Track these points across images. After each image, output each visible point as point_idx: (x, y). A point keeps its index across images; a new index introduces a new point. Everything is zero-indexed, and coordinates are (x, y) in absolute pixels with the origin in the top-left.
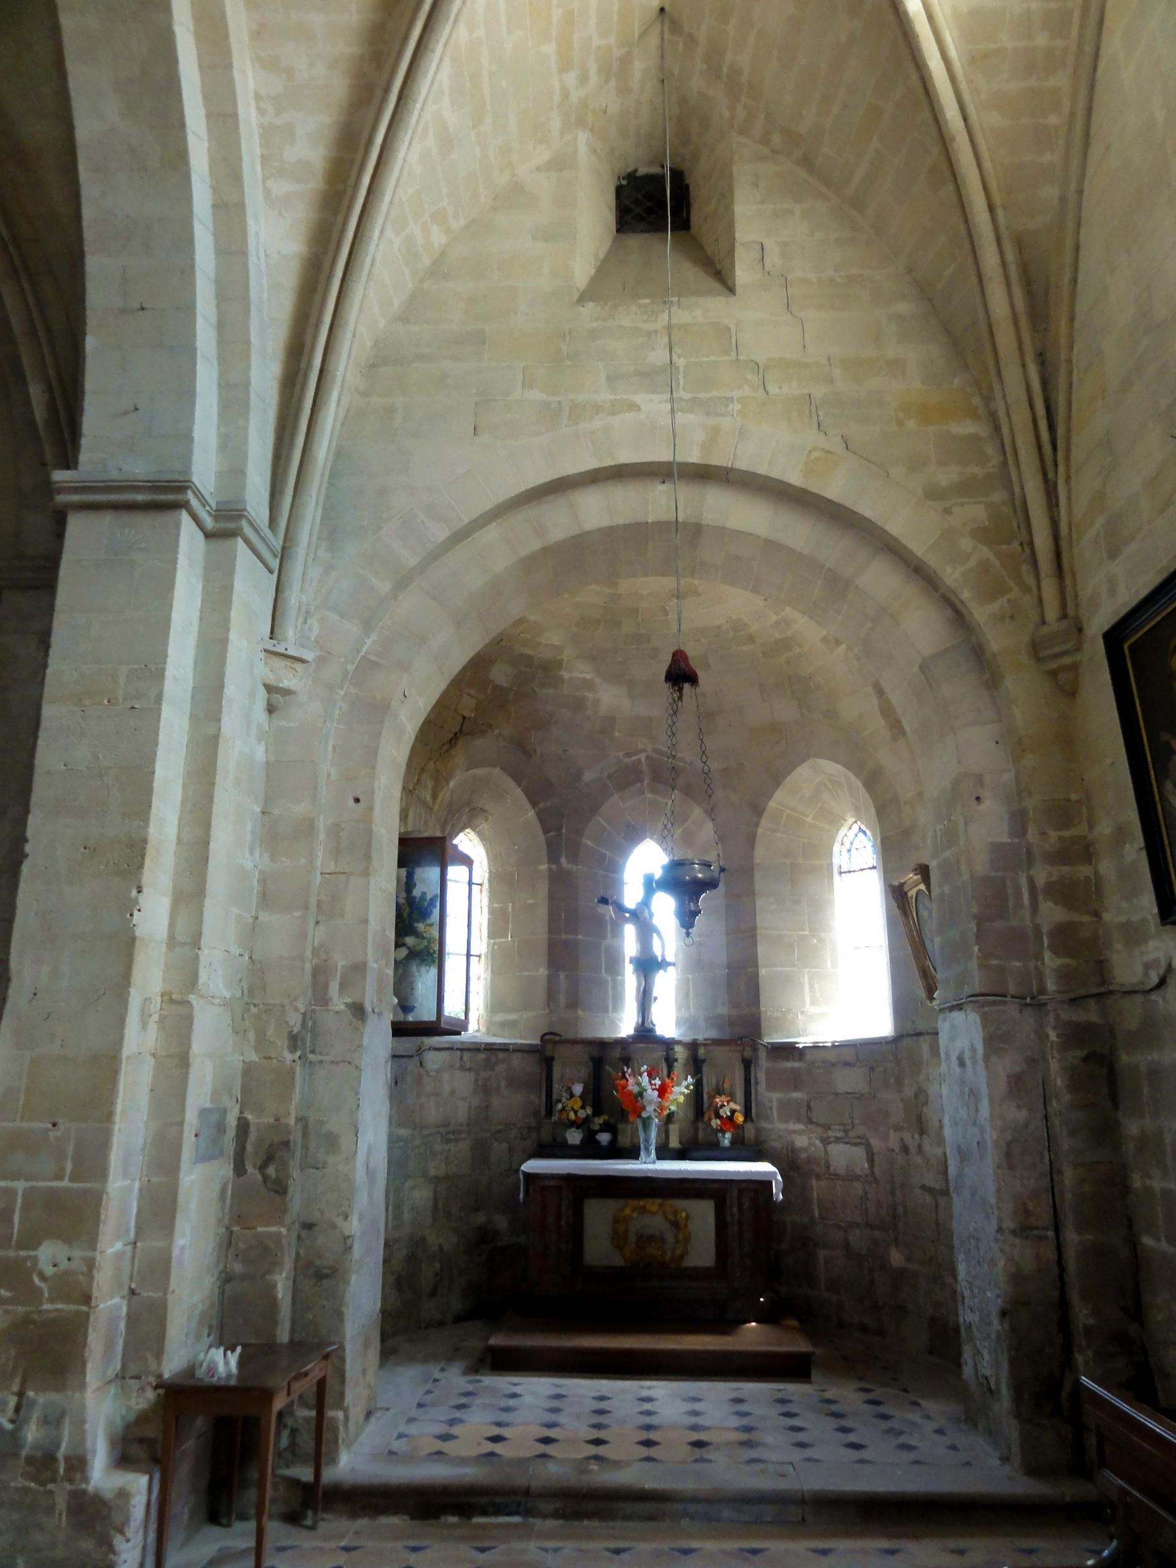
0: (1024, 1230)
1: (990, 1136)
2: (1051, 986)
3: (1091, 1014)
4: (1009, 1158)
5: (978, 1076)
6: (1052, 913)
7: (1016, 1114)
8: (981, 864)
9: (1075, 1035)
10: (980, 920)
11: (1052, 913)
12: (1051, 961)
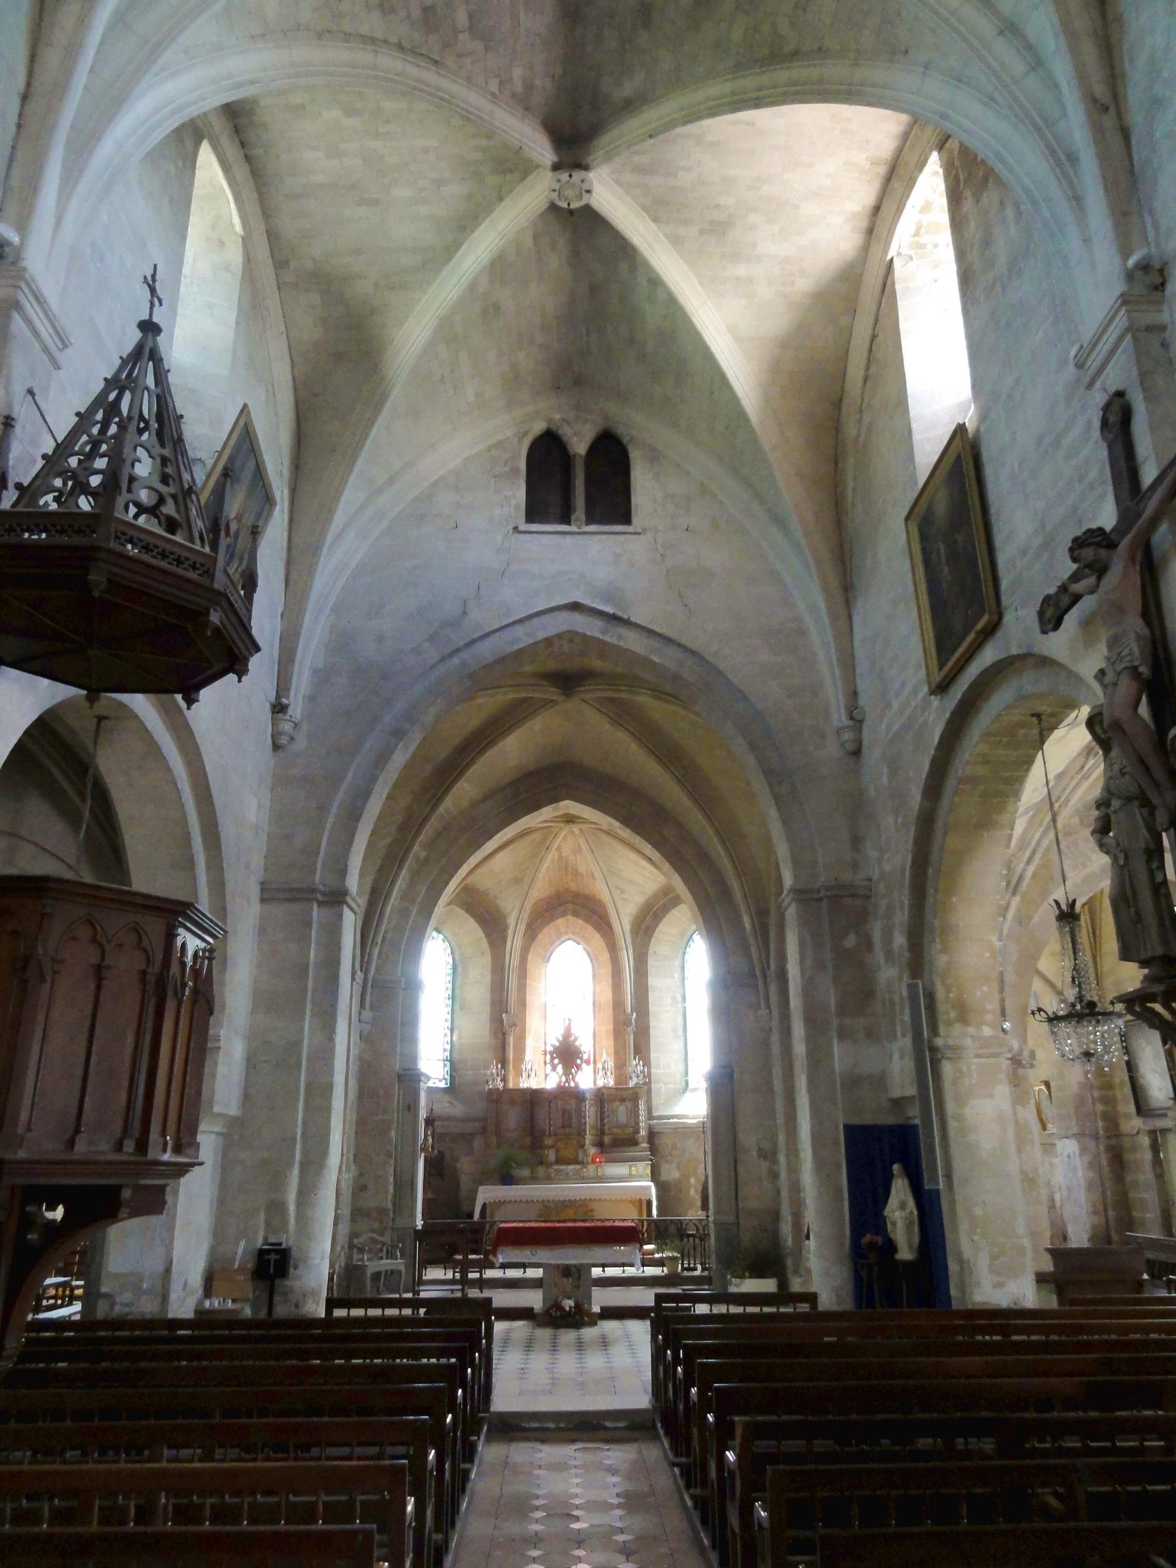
0: (1095, 1213)
1: (1082, 1182)
3: (1114, 1142)
4: (1090, 1186)
6: (1100, 1108)
7: (1091, 1174)
9: (1110, 1149)
10: (1077, 1108)
11: (1100, 1108)
12: (1100, 1124)
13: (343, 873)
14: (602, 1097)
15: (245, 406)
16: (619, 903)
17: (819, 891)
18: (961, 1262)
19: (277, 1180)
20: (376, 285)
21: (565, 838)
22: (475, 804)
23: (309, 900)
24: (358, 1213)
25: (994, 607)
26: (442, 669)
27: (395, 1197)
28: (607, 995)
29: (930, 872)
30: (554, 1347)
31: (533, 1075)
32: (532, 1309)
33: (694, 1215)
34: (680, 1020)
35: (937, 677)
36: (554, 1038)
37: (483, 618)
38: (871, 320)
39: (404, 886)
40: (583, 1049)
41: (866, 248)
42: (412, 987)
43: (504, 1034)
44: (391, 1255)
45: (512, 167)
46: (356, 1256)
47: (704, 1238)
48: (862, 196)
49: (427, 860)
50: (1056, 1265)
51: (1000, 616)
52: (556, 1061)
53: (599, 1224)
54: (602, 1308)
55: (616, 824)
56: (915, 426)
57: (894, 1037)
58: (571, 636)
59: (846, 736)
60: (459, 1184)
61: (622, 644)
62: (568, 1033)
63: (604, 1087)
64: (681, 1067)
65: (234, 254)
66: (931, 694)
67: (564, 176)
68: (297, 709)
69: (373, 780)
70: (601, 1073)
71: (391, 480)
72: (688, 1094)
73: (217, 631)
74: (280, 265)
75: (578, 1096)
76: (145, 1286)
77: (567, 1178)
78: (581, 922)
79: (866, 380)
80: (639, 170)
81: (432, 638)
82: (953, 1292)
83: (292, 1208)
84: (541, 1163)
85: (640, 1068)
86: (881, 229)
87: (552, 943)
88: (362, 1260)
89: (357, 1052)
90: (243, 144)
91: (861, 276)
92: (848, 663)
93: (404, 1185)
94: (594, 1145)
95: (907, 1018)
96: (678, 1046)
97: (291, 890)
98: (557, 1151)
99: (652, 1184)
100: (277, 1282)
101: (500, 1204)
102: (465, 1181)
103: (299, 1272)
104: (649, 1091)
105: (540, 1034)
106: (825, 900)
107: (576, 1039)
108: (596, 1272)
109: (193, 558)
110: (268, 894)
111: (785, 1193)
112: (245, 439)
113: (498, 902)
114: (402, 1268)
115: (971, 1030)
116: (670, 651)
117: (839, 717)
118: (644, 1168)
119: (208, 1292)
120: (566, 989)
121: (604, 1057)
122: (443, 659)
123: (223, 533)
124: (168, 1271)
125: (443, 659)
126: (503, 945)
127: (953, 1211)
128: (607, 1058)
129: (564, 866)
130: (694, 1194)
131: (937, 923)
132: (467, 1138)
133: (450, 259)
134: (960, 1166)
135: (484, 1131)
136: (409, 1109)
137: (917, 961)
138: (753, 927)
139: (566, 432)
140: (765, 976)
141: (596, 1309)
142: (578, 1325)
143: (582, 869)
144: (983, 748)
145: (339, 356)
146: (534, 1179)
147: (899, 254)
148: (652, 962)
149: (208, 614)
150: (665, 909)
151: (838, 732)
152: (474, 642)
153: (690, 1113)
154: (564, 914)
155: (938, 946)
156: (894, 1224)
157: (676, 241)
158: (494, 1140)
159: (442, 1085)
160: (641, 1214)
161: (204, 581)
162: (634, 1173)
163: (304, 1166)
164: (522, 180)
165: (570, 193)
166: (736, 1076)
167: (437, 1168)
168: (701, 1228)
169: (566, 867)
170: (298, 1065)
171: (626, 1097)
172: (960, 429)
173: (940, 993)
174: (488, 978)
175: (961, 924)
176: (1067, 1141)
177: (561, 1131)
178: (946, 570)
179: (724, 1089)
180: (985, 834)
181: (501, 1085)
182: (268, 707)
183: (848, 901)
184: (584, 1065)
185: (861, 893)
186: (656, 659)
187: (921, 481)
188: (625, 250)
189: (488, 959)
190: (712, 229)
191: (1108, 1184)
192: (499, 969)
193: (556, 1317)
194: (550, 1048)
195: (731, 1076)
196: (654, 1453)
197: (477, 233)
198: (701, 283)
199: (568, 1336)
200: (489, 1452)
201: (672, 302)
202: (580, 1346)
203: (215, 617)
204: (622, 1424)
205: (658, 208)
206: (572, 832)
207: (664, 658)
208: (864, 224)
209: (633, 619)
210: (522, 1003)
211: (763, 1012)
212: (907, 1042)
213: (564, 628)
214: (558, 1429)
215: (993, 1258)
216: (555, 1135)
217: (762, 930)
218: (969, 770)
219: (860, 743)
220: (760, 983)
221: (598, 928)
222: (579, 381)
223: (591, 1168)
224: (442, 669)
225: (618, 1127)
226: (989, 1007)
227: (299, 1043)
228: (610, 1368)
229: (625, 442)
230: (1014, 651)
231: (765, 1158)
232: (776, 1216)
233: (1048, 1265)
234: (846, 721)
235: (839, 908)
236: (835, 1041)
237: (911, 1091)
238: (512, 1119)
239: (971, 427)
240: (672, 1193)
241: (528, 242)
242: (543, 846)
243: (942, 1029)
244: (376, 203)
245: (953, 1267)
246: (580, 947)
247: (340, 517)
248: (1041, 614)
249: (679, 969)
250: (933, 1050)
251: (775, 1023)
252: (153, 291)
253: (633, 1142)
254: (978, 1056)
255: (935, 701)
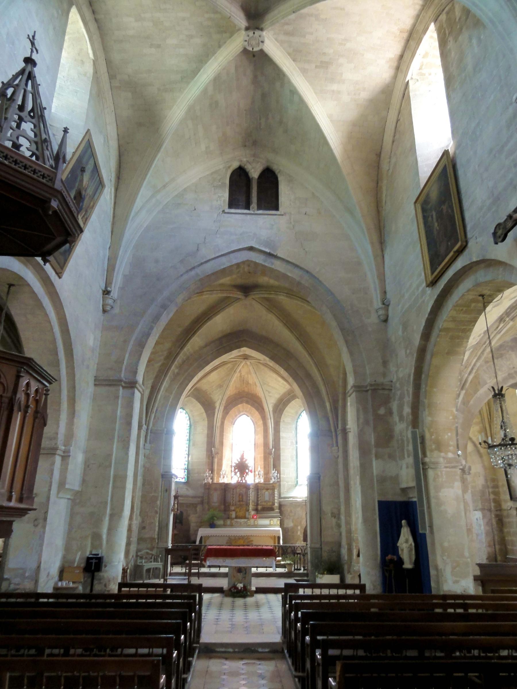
0: (489, 546)
1: (484, 532)
2: (493, 508)
3: (498, 513)
4: (487, 534)
5: (481, 522)
6: (492, 497)
7: (487, 528)
8: (480, 487)
9: (497, 516)
11: (492, 497)
12: (493, 504)
13: (135, 373)
14: (257, 487)
15: (88, 130)
16: (268, 398)
17: (366, 387)
18: (436, 568)
19: (98, 522)
20: (159, 89)
21: (243, 367)
22: (202, 348)
23: (119, 385)
24: (140, 540)
25: (463, 237)
26: (185, 277)
27: (159, 532)
28: (261, 441)
29: (423, 376)
30: (233, 608)
31: (226, 477)
32: (222, 588)
33: (300, 543)
34: (295, 453)
35: (430, 278)
36: (236, 460)
37: (206, 253)
38: (397, 112)
39: (167, 386)
40: (249, 465)
41: (395, 77)
42: (169, 433)
43: (213, 458)
44: (156, 560)
45: (227, 30)
46: (139, 561)
47: (305, 555)
48: (394, 49)
49: (177, 373)
50: (481, 571)
51: (467, 242)
52: (237, 470)
53: (255, 547)
54: (256, 588)
55: (267, 359)
56: (419, 159)
57: (402, 458)
58: (248, 263)
59: (381, 312)
60: (189, 527)
61: (273, 267)
62: (242, 458)
63: (259, 483)
64: (295, 475)
65: (89, 69)
66: (427, 287)
67: (251, 33)
68: (115, 293)
69: (151, 328)
70: (257, 477)
71: (164, 186)
72: (297, 487)
73: (55, 212)
74: (112, 77)
75: (246, 487)
76: (27, 575)
77: (240, 525)
78: (249, 406)
79: (393, 142)
80: (287, 33)
81: (182, 261)
82: (433, 584)
83: (104, 537)
84: (229, 518)
85: (276, 474)
86: (403, 67)
87: (236, 416)
88: (142, 562)
89: (143, 463)
90: (94, 12)
91: (393, 91)
92: (382, 278)
93: (163, 527)
94: (253, 510)
95: (411, 448)
96: (293, 464)
97: (110, 380)
98: (236, 513)
99: (280, 529)
100: (96, 574)
101: (208, 537)
102: (193, 525)
103: (107, 568)
104: (280, 485)
105: (229, 458)
106: (370, 392)
107: (246, 460)
108: (254, 570)
109: (44, 171)
110: (98, 382)
111: (344, 534)
112: (88, 148)
113: (212, 396)
114: (161, 567)
115: (442, 454)
116: (297, 271)
117: (377, 303)
118: (276, 521)
119: (61, 579)
120: (242, 437)
121: (259, 469)
122: (187, 272)
123: (61, 161)
124: (39, 567)
125: (187, 272)
126: (213, 416)
127: (433, 544)
128: (260, 470)
129: (243, 381)
130: (300, 534)
131: (426, 401)
132: (194, 506)
133: (195, 76)
134: (437, 522)
135: (202, 503)
136: (166, 491)
137: (416, 421)
138: (331, 408)
139: (249, 168)
140: (336, 431)
141: (253, 589)
142: (244, 596)
143: (251, 382)
144: (454, 313)
145: (140, 125)
146: (225, 526)
147: (412, 78)
148: (282, 425)
149: (50, 202)
150: (289, 401)
151: (377, 311)
152: (202, 264)
153: (299, 496)
154: (242, 402)
155: (426, 412)
156: (402, 550)
157: (304, 71)
158: (206, 506)
159: (183, 480)
160: (275, 543)
161: (49, 184)
162: (272, 523)
163: (112, 516)
164: (230, 37)
165: (253, 42)
166: (321, 478)
167: (179, 520)
168: (303, 550)
169: (243, 381)
170: (111, 466)
171: (269, 487)
172: (446, 153)
173: (427, 436)
174: (206, 432)
175: (438, 402)
176: (476, 512)
177: (238, 503)
178: (436, 224)
179: (316, 485)
180: (451, 358)
181: (210, 481)
182: (101, 292)
183: (381, 392)
184: (250, 473)
185: (387, 388)
186: (289, 274)
187: (422, 186)
188: (279, 74)
189: (206, 423)
190: (322, 66)
191: (496, 533)
192: (211, 428)
193: (234, 592)
194: (234, 465)
195: (319, 478)
196: (283, 666)
197: (207, 64)
198: (316, 93)
199: (240, 601)
200: (198, 664)
201: (302, 102)
202: (245, 607)
203: (54, 204)
204: (267, 650)
205: (296, 54)
206: (247, 364)
207: (294, 274)
208: (395, 64)
209: (279, 255)
210: (222, 443)
211: (335, 448)
212: (410, 460)
213: (245, 259)
214: (234, 652)
215: (454, 568)
216: (236, 505)
217: (335, 409)
218: (446, 325)
219: (388, 316)
220: (334, 434)
221: (258, 410)
222: (255, 143)
223: (252, 521)
224: (185, 277)
225: (265, 502)
226: (451, 443)
227: (110, 456)
228: (261, 619)
229: (276, 172)
230: (474, 260)
231: (335, 517)
232: (340, 545)
233: (478, 572)
234: (380, 305)
235: (376, 395)
236: (374, 459)
237: (412, 484)
238: (216, 497)
239: (451, 152)
240: (290, 534)
241: (233, 70)
242: (232, 370)
243: (428, 453)
244: (159, 46)
245: (432, 572)
246: (249, 418)
247: (139, 202)
248: (495, 234)
249: (295, 429)
250: (424, 464)
251: (341, 454)
252: (33, 44)
253: (271, 509)
254: (446, 467)
255: (429, 290)
